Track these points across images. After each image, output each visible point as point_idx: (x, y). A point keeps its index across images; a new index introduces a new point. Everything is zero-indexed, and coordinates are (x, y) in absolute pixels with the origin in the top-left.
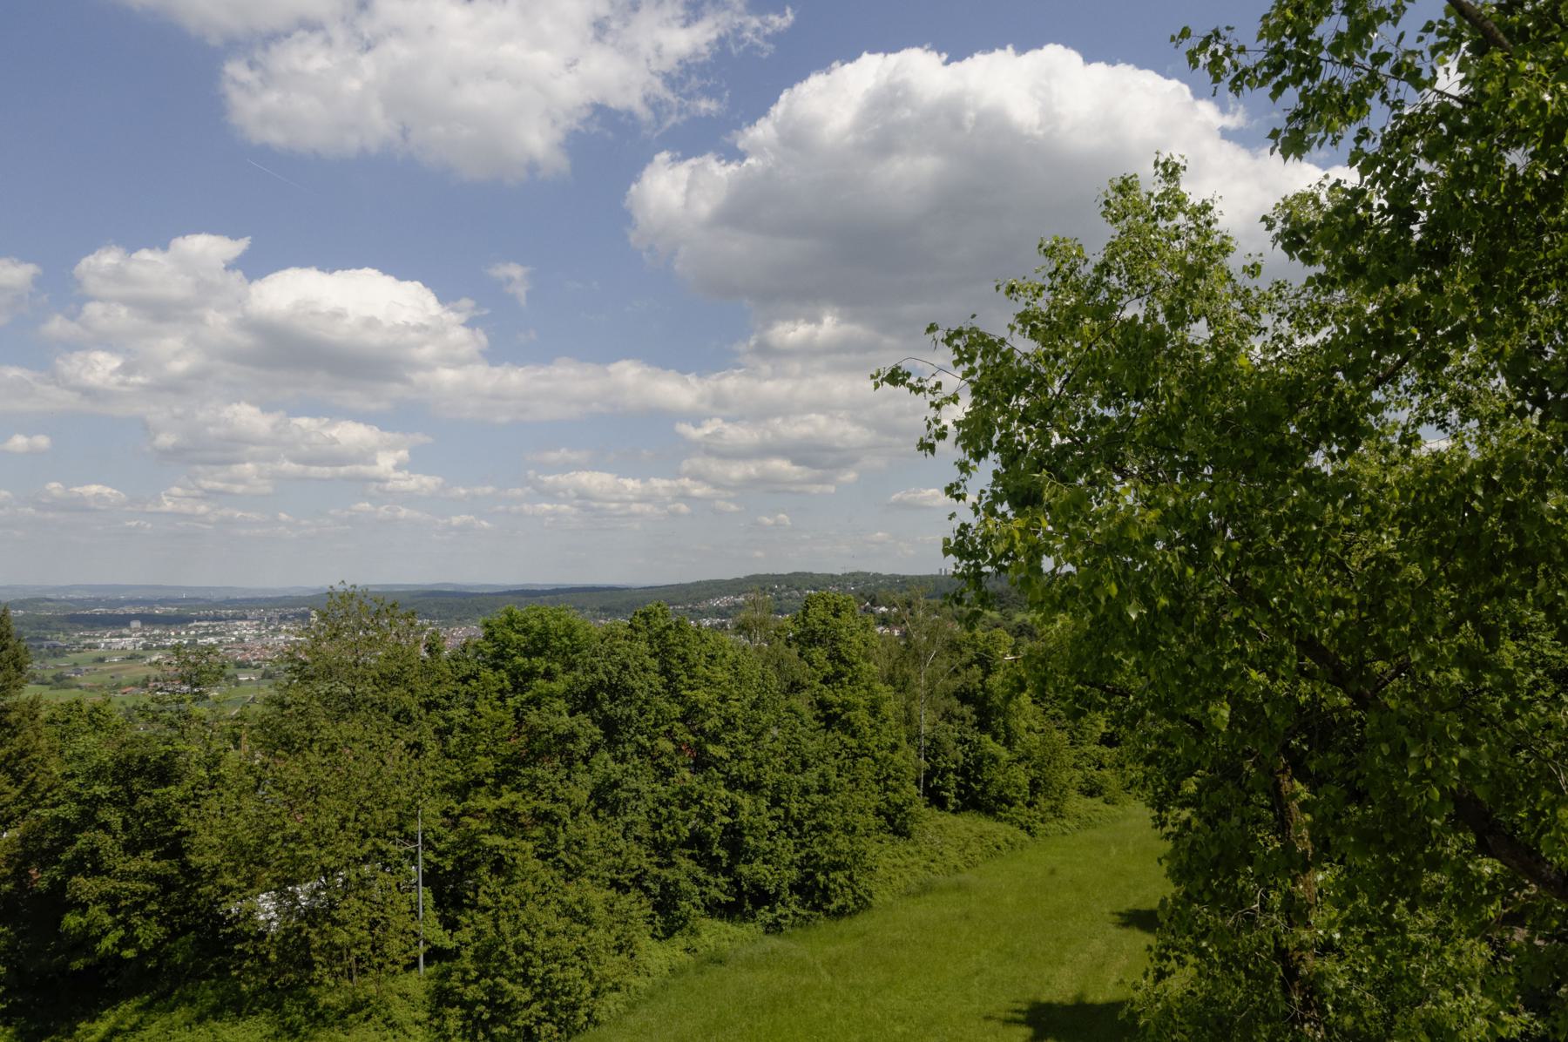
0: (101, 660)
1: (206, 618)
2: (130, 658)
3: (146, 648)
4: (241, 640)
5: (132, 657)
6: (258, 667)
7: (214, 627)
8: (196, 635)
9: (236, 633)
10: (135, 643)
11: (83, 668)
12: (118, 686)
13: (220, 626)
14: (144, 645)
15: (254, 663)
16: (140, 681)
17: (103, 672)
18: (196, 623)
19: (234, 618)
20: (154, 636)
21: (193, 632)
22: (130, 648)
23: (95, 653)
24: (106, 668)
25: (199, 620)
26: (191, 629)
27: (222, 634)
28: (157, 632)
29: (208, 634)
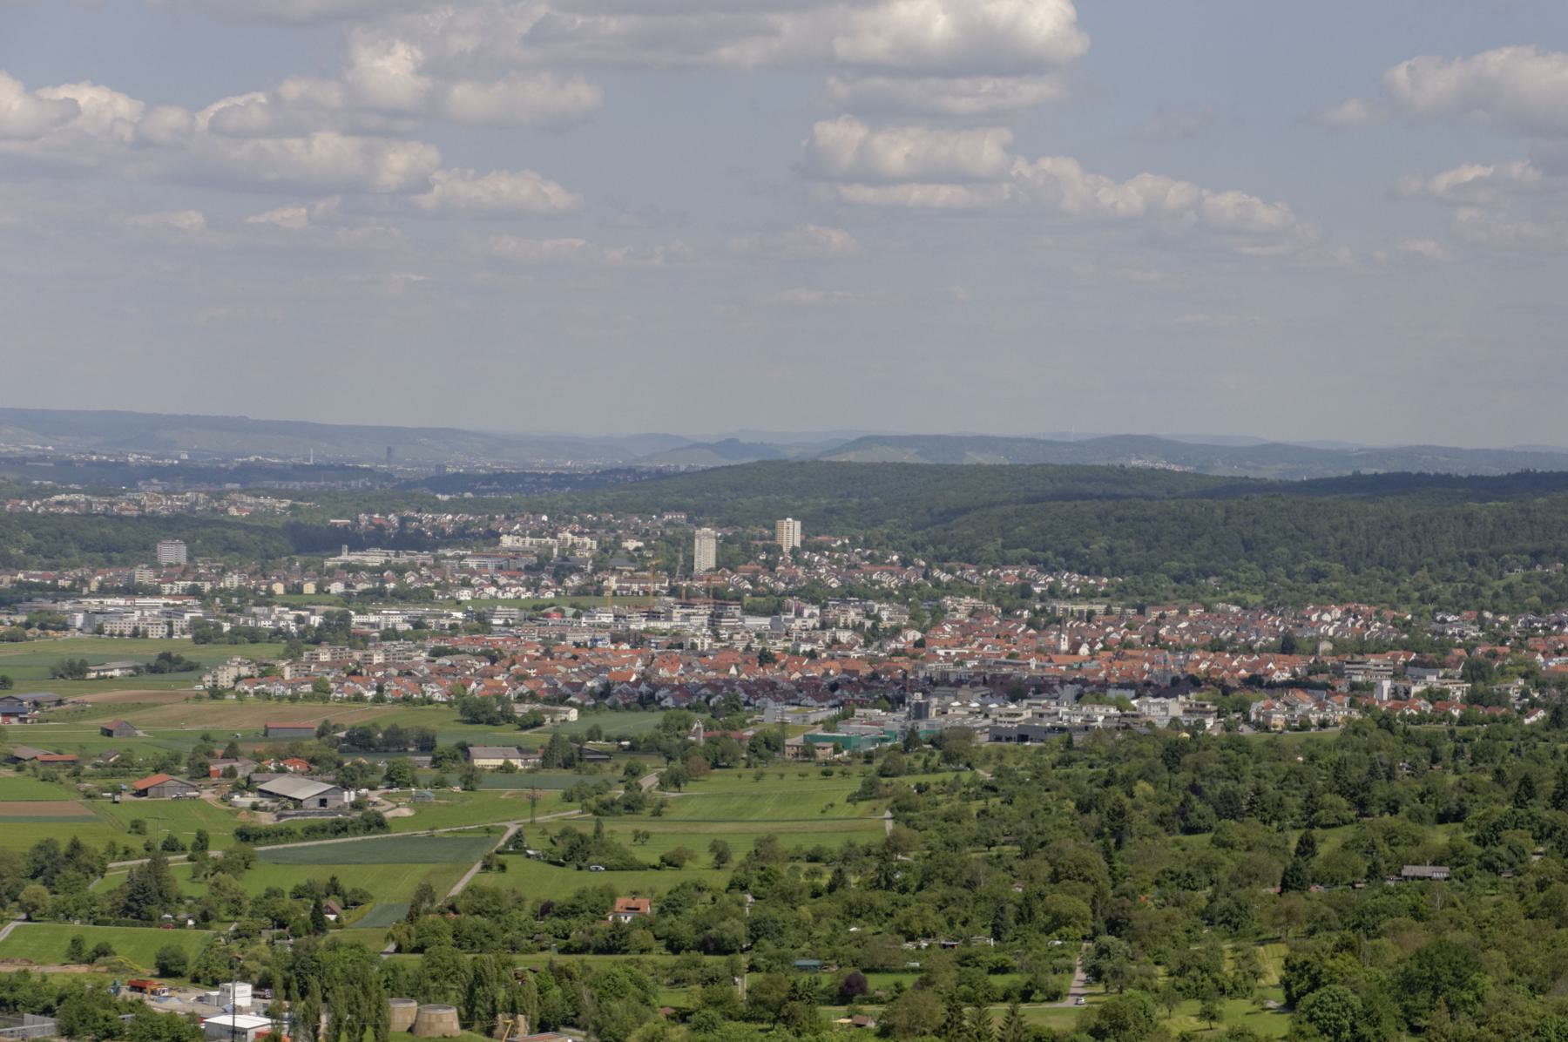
0: (75, 671)
1: (376, 539)
2: (154, 670)
3: (203, 634)
4: (480, 622)
5: (167, 664)
6: (533, 723)
7: (400, 571)
8: (347, 598)
9: (465, 595)
10: (172, 613)
11: (27, 697)
12: (124, 766)
13: (418, 568)
14: (195, 625)
15: (521, 710)
16: (187, 750)
17: (81, 712)
18: (346, 557)
19: (461, 537)
20: (226, 593)
21: (337, 588)
22: (158, 632)
23: (58, 646)
24: (90, 698)
25: (358, 545)
26: (331, 574)
27: (423, 596)
28: (233, 581)
29: (377, 596)
